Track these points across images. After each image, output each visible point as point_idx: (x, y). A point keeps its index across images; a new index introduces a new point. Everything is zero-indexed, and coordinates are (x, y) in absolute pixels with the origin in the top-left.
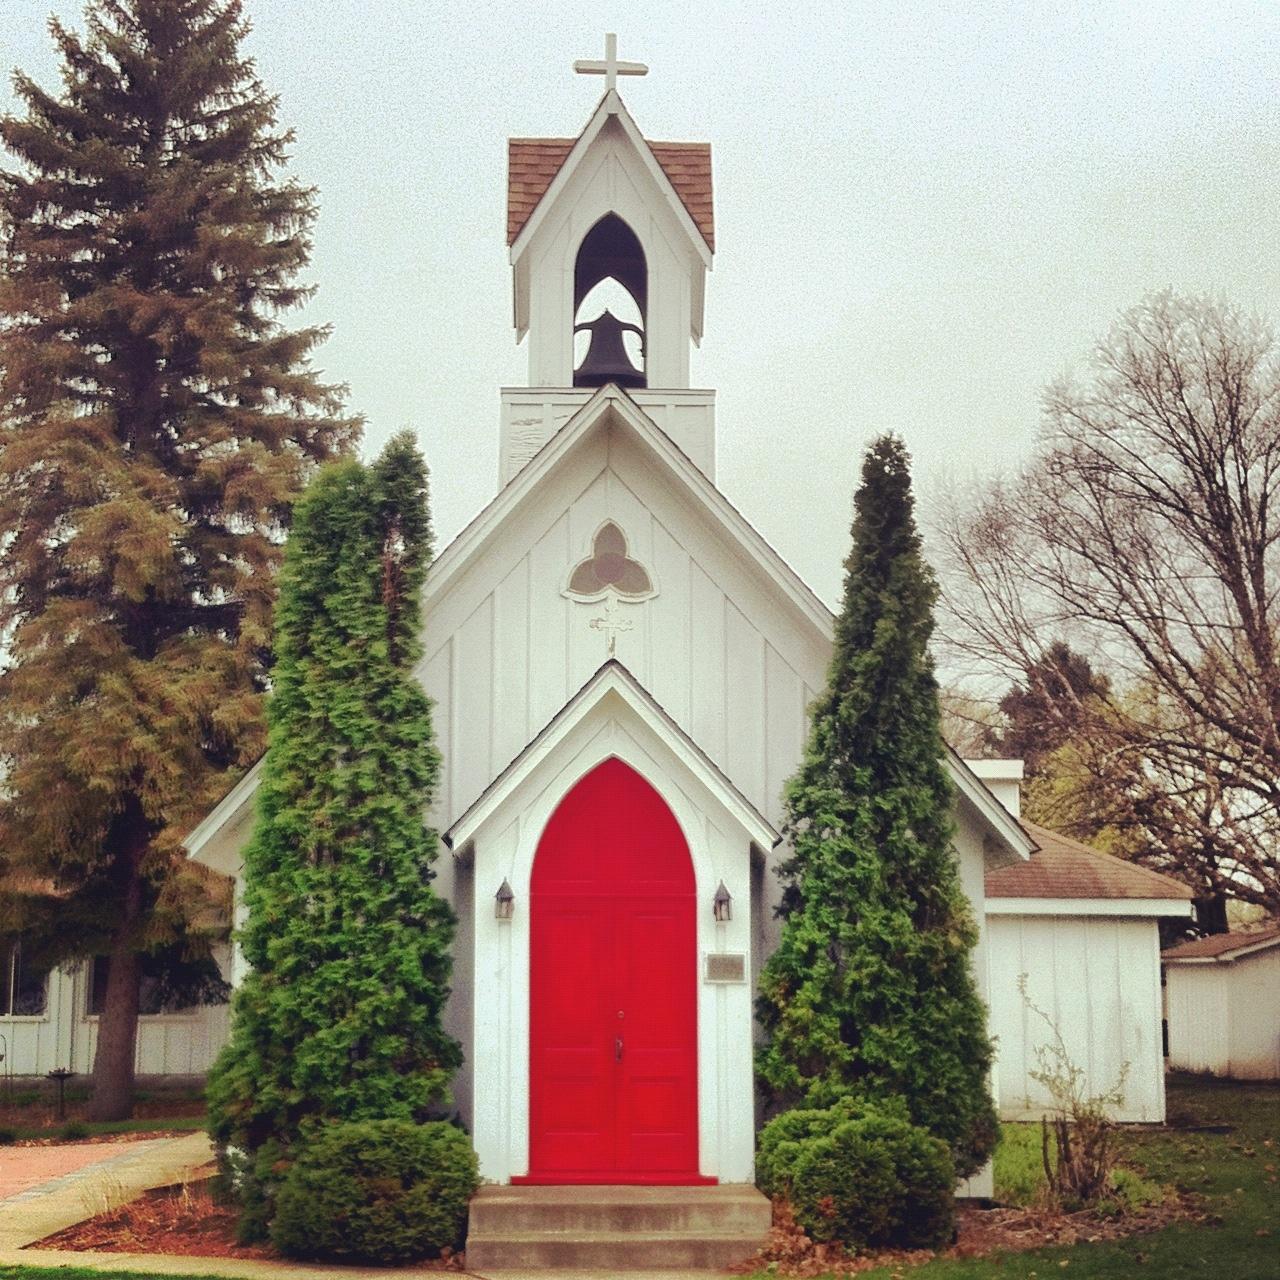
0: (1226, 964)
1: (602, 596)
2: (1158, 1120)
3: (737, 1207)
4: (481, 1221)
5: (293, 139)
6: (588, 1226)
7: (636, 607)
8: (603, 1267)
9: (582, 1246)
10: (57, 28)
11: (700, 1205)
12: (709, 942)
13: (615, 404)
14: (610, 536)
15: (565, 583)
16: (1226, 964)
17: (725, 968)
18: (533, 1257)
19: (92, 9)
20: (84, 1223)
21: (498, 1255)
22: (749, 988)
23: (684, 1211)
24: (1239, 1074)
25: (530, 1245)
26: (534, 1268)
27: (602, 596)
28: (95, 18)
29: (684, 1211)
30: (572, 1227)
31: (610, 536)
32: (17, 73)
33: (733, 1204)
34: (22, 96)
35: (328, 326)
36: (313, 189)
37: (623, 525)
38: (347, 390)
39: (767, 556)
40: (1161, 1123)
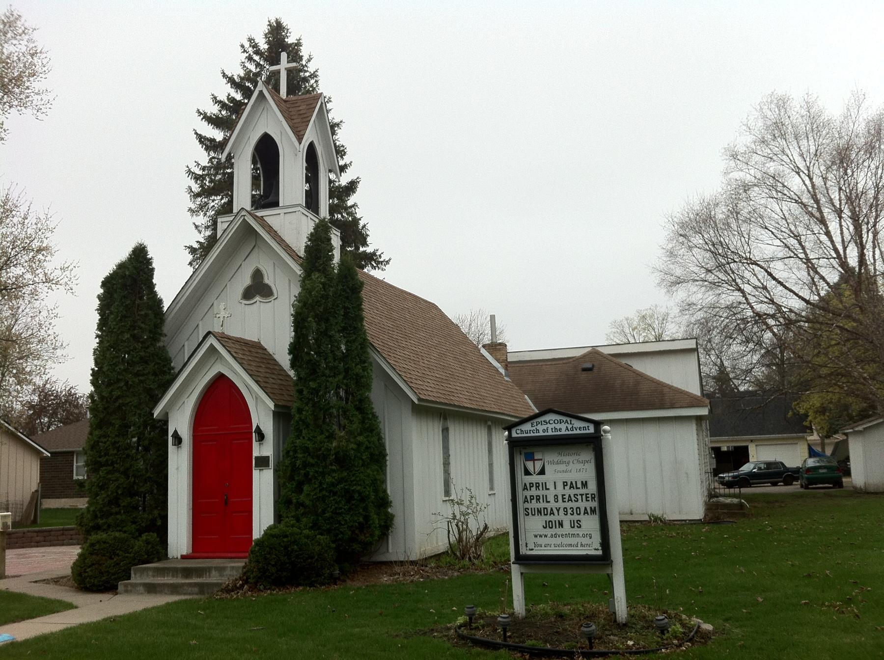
0: (860, 432)
1: (255, 300)
2: (698, 518)
3: (229, 569)
4: (135, 574)
5: (330, 101)
6: (173, 576)
7: (255, 305)
8: (165, 594)
9: (159, 585)
10: (224, 75)
11: (215, 568)
12: (258, 451)
13: (246, 218)
14: (258, 275)
15: (240, 297)
16: (860, 432)
17: (263, 462)
18: (141, 589)
19: (243, 63)
20: (63, 577)
21: (129, 588)
22: (272, 471)
23: (208, 570)
24: (872, 490)
25: (140, 584)
26: (142, 593)
27: (255, 300)
28: (244, 66)
29: (208, 570)
30: (167, 576)
31: (258, 275)
32: (213, 95)
33: (227, 567)
34: (216, 105)
35: (358, 178)
36: (341, 122)
37: (262, 268)
38: (357, 206)
39: (185, 290)
40: (701, 520)
